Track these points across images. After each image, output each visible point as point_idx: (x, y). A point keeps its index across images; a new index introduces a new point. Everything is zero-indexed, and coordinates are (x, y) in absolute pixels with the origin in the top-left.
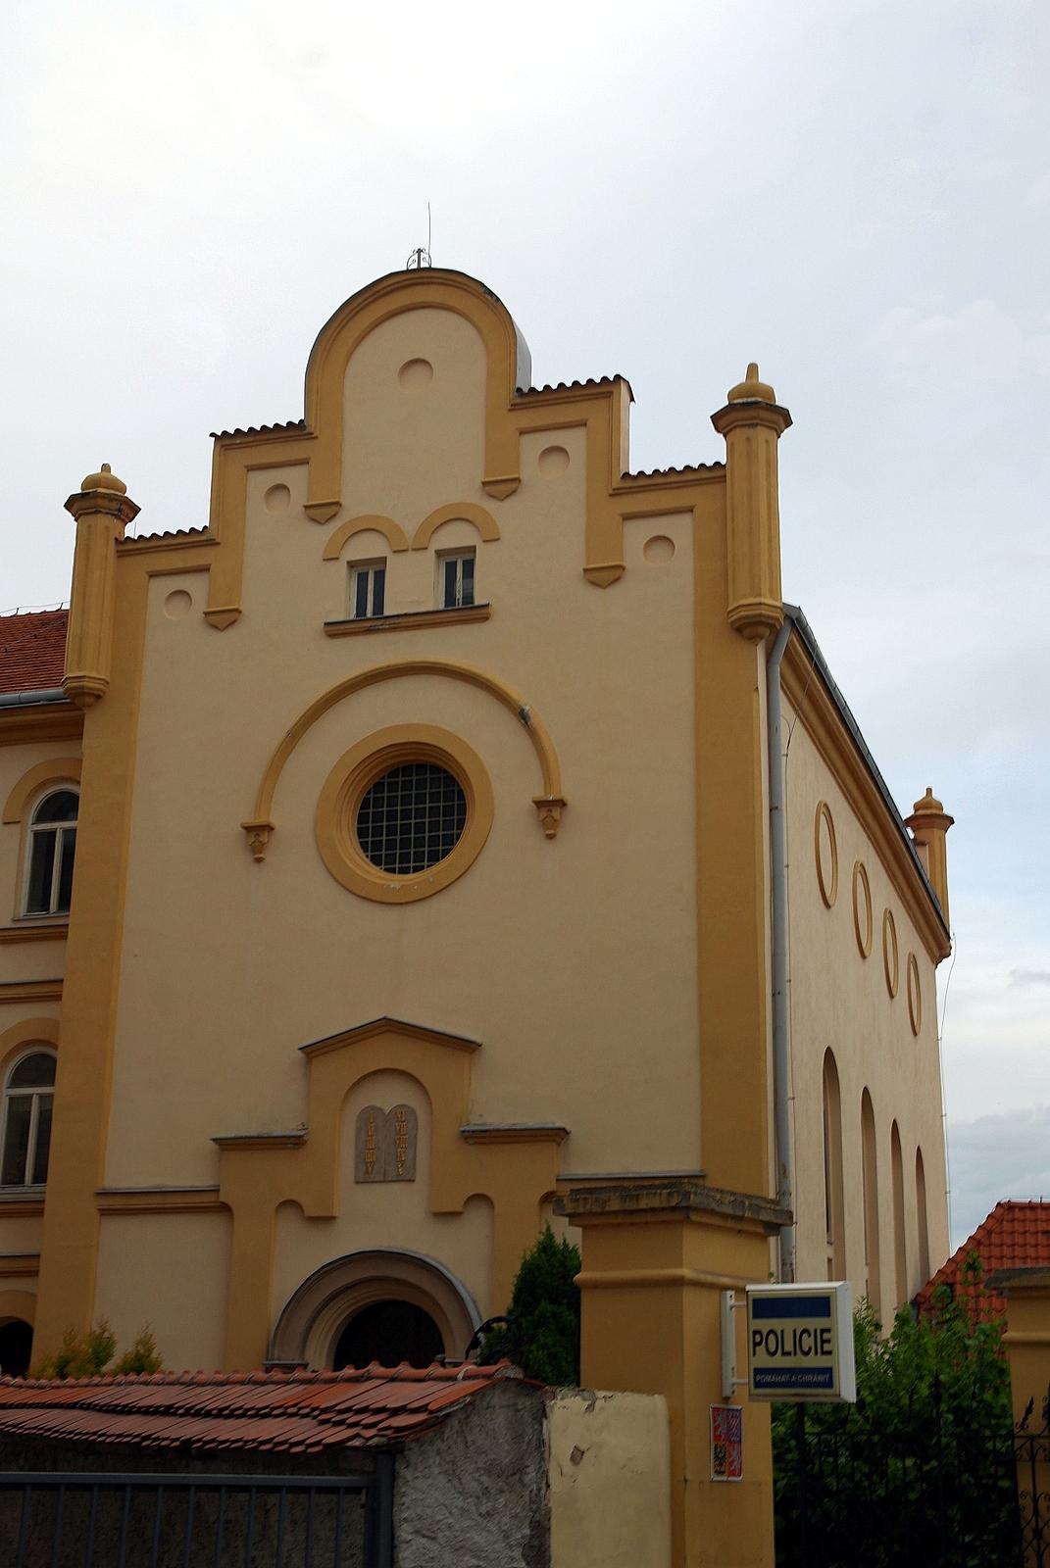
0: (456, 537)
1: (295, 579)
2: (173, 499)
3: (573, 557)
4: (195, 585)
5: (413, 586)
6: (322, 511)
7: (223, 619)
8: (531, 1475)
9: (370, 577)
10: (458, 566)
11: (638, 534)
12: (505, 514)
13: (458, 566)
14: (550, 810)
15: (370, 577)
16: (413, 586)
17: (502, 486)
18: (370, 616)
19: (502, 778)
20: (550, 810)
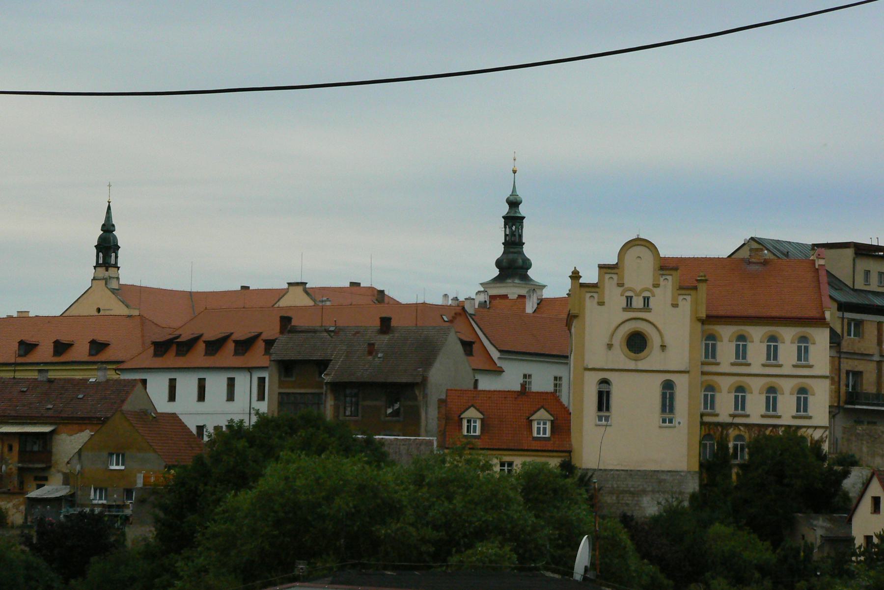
0: (647, 294)
1: (615, 298)
2: (590, 276)
3: (669, 301)
4: (595, 295)
5: (638, 303)
6: (621, 285)
7: (601, 303)
8: (664, 477)
9: (629, 299)
10: (646, 300)
11: (681, 297)
12: (655, 290)
13: (646, 300)
14: (663, 347)
15: (629, 299)
16: (638, 303)
17: (656, 286)
18: (629, 306)
19: (655, 340)
20: (663, 347)
